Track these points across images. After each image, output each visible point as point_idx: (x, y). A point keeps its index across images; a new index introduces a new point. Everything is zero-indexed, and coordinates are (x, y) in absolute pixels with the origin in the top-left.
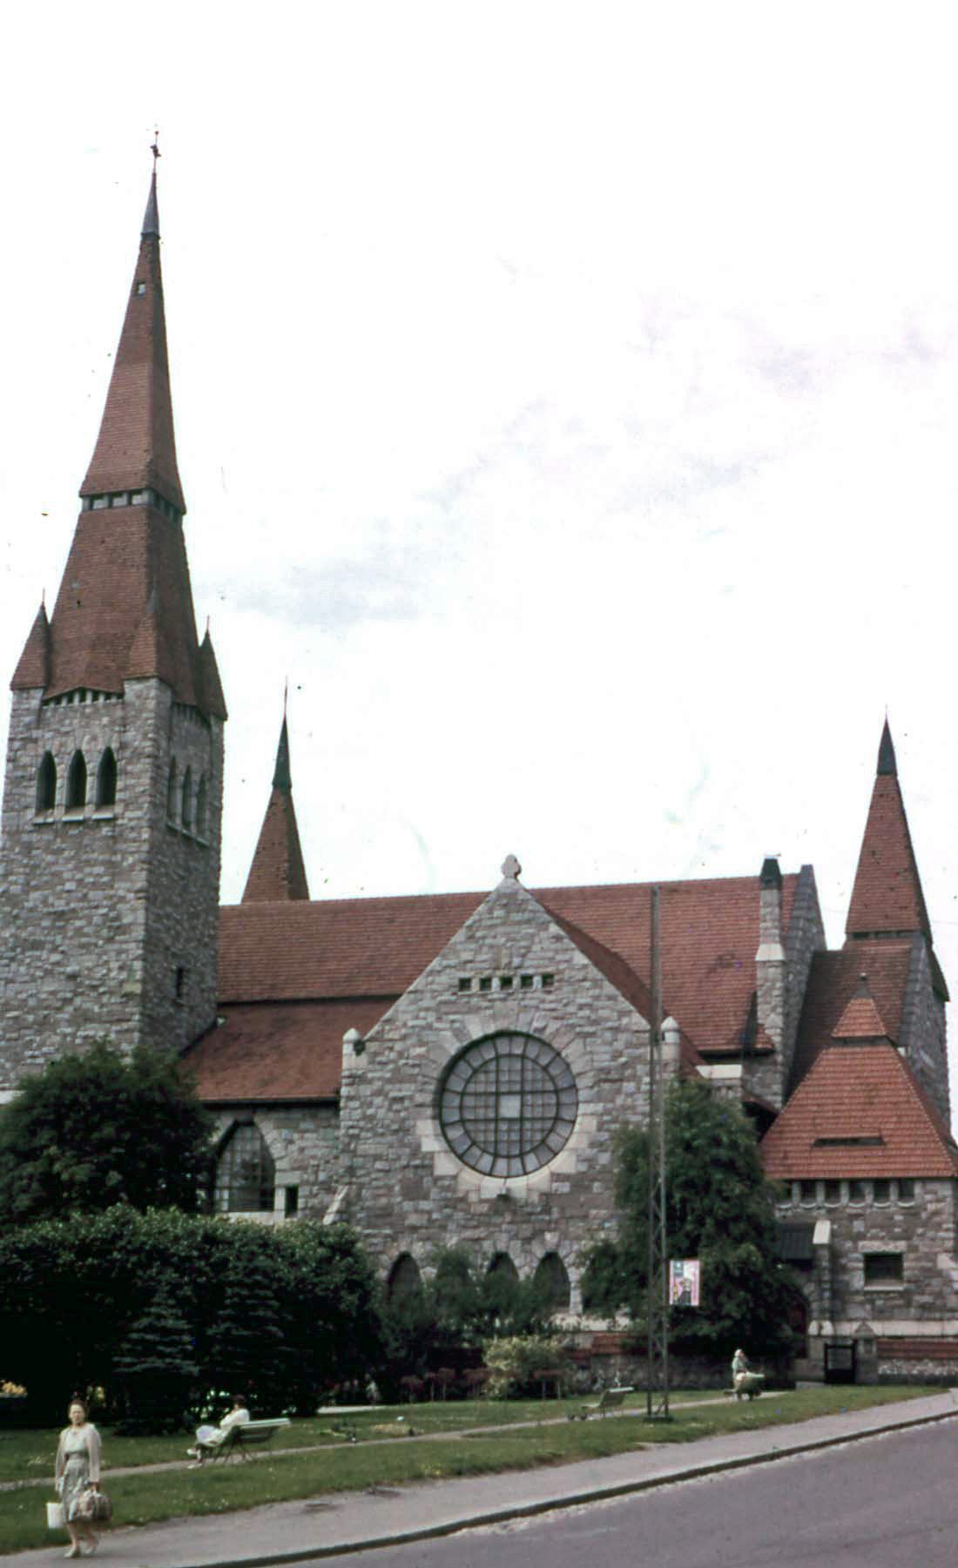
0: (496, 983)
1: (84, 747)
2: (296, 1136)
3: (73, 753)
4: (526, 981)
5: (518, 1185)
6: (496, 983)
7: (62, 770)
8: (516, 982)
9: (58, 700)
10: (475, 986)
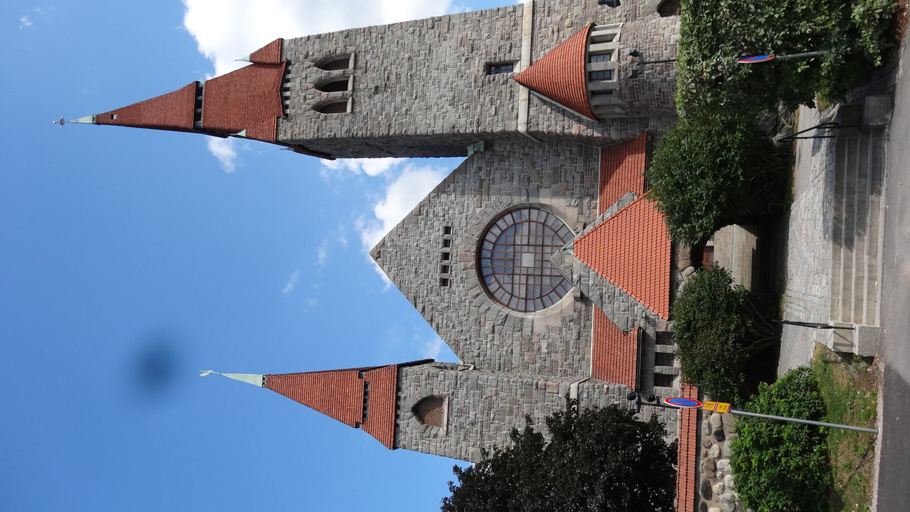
9: (287, 107)
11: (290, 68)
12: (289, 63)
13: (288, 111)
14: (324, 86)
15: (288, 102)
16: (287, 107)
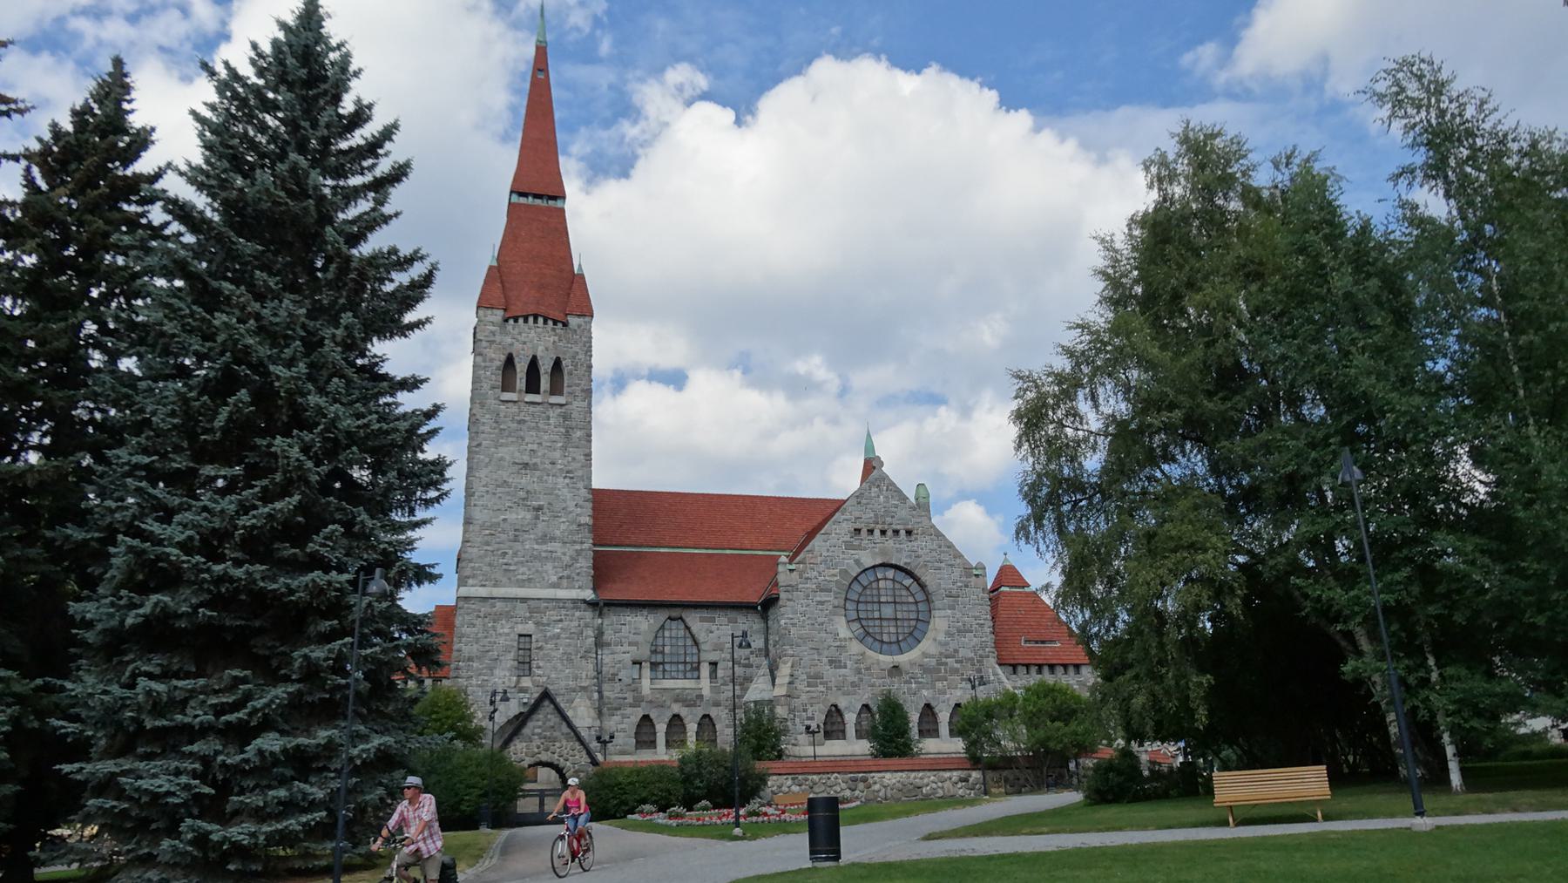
0: (877, 533)
1: (539, 355)
2: (714, 628)
4: (896, 532)
5: (901, 659)
6: (877, 533)
7: (521, 367)
8: (889, 533)
9: (516, 321)
10: (864, 532)
11: (560, 325)
13: (511, 321)
14: (533, 365)
15: (521, 321)
16: (516, 321)
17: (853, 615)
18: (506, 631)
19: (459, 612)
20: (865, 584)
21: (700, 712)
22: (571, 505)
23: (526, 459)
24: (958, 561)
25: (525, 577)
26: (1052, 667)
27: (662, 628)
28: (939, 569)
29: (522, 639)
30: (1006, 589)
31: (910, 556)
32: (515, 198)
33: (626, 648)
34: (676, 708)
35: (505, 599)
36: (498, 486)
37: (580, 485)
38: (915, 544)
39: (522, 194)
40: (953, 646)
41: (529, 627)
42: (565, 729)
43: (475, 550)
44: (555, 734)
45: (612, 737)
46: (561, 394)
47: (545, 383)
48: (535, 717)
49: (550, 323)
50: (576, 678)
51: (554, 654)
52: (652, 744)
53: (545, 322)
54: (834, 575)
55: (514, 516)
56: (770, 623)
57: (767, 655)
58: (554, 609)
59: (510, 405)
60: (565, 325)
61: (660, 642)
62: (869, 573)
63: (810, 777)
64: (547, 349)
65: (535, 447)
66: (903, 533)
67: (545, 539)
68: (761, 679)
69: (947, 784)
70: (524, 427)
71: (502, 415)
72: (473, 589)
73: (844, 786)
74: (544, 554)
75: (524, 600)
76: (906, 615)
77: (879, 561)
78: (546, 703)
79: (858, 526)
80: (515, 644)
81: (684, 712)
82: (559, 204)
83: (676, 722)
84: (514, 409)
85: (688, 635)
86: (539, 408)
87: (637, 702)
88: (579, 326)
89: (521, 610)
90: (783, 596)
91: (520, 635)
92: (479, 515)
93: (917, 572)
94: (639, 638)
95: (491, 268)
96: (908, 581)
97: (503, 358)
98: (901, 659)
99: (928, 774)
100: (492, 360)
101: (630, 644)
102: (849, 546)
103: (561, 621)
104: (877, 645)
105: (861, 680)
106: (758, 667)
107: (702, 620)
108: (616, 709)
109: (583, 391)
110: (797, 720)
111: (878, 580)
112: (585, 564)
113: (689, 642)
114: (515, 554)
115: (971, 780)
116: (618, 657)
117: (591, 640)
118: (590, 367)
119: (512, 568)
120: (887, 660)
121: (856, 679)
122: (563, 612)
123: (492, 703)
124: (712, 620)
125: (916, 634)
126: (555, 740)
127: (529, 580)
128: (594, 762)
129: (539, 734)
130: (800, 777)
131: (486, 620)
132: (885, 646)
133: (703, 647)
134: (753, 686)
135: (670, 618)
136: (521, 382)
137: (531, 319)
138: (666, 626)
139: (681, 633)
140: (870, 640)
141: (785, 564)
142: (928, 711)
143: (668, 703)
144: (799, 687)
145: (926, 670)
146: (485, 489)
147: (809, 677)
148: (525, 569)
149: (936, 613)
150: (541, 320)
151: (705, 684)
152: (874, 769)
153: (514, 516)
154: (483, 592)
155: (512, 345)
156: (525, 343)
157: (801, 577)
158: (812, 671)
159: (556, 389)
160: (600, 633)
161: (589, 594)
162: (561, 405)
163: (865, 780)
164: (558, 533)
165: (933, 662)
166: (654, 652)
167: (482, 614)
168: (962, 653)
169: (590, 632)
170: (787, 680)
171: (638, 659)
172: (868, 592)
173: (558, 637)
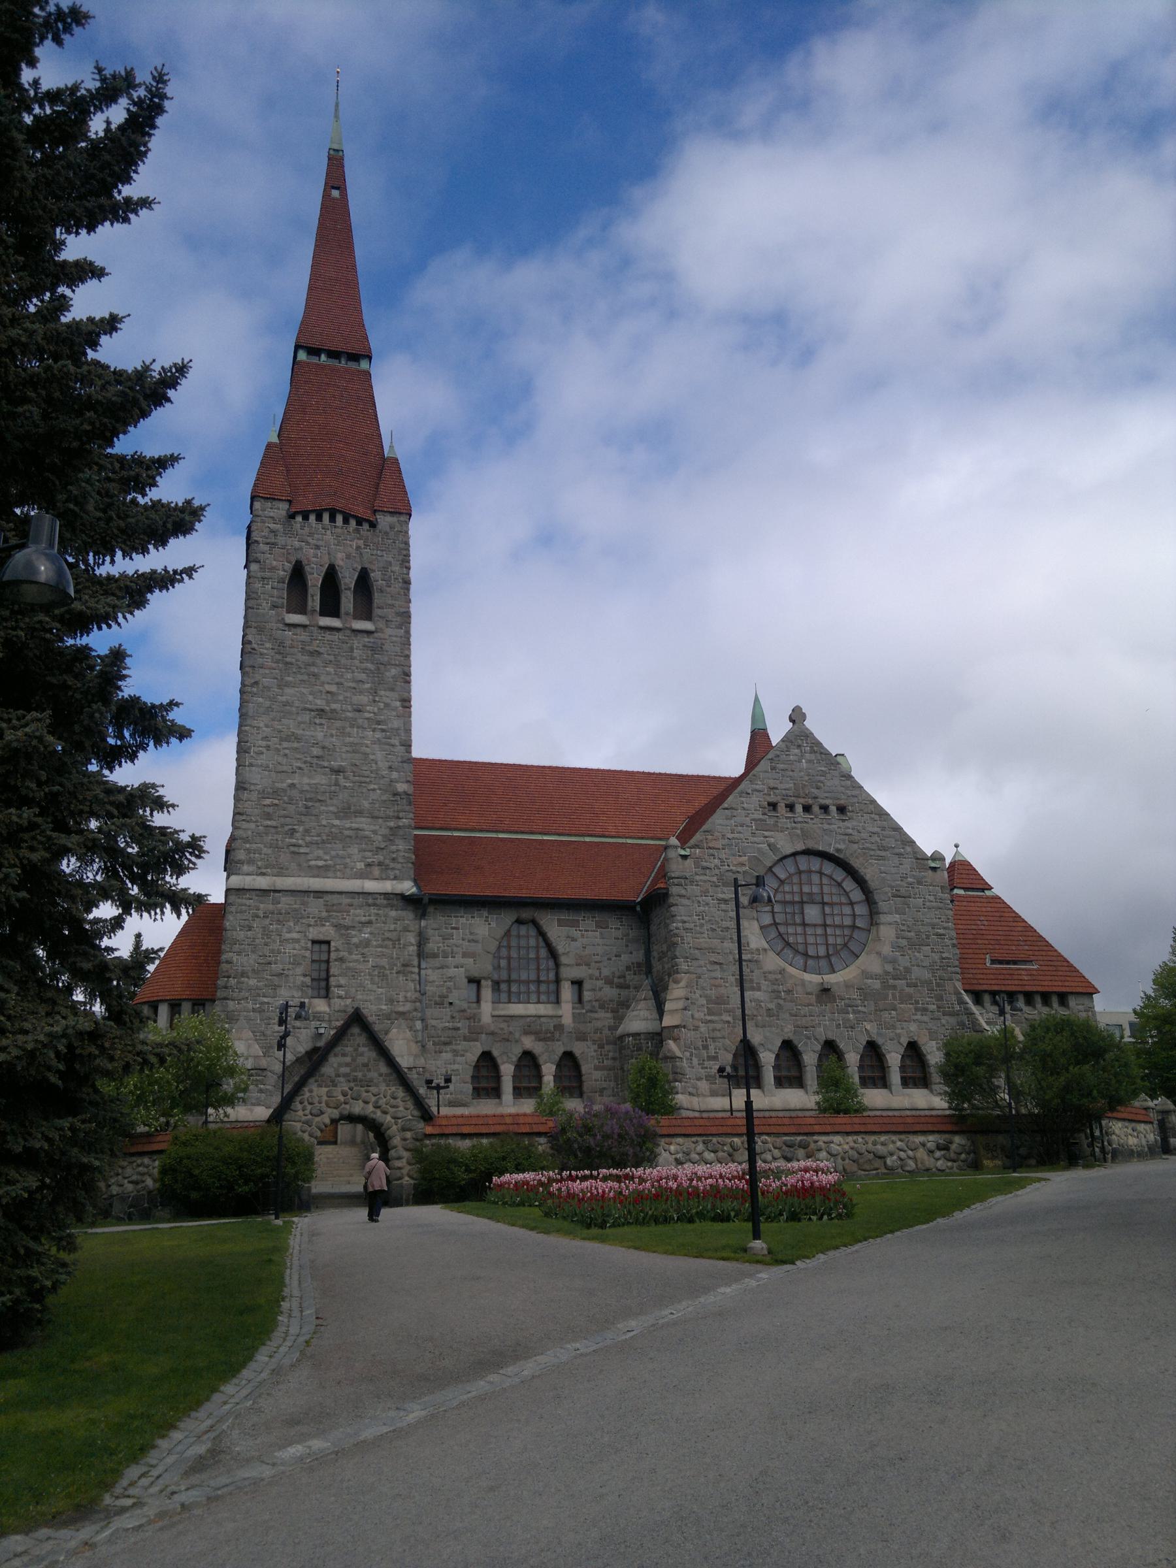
0: (799, 808)
2: (577, 934)
3: (327, 566)
5: (831, 979)
6: (799, 808)
7: (315, 580)
8: (816, 809)
11: (366, 526)
12: (373, 525)
13: (299, 519)
14: (331, 578)
15: (312, 518)
17: (767, 919)
18: (295, 935)
19: (229, 909)
20: (783, 876)
21: (559, 1049)
22: (383, 765)
23: (320, 703)
24: (909, 849)
25: (320, 863)
26: (1029, 997)
27: (508, 934)
28: (883, 858)
29: (316, 947)
30: (961, 892)
31: (844, 841)
32: (302, 356)
33: (459, 959)
34: (528, 1043)
35: (293, 892)
36: (282, 740)
37: (396, 741)
38: (846, 823)
39: (314, 351)
40: (904, 962)
41: (326, 931)
42: (383, 1068)
43: (253, 826)
44: (373, 1075)
45: (448, 1080)
46: (368, 617)
47: (347, 601)
48: (338, 1049)
49: (353, 522)
50: (391, 1001)
51: (361, 967)
52: (496, 1092)
53: (346, 521)
54: (744, 865)
55: (306, 780)
56: (653, 928)
57: (649, 972)
58: (360, 907)
59: (299, 630)
60: (373, 525)
61: (504, 952)
62: (789, 861)
63: (729, 1140)
64: (348, 557)
65: (333, 688)
66: (833, 809)
67: (346, 812)
68: (642, 1005)
69: (921, 1154)
70: (318, 661)
71: (288, 643)
72: (248, 879)
73: (777, 1153)
74: (347, 833)
75: (319, 894)
76: (838, 920)
77: (800, 847)
78: (356, 1030)
79: (772, 799)
80: (308, 954)
81: (537, 1048)
82: (364, 365)
83: (529, 1062)
84: (303, 636)
85: (542, 944)
86: (336, 637)
87: (474, 1034)
88: (392, 527)
89: (315, 907)
90: (674, 890)
91: (314, 942)
92: (256, 777)
93: (856, 863)
94: (478, 948)
95: (269, 446)
96: (839, 874)
97: (289, 567)
98: (831, 979)
99: (894, 1138)
100: (273, 569)
101: (465, 955)
102: (761, 825)
103: (370, 922)
104: (800, 960)
105: (779, 1006)
106: (637, 988)
107: (561, 923)
108: (446, 1044)
109: (398, 614)
110: (695, 1061)
111: (800, 872)
112: (402, 847)
113: (543, 952)
114: (307, 831)
115: (953, 1147)
116: (452, 972)
117: (413, 949)
118: (407, 582)
119: (302, 850)
120: (813, 979)
121: (772, 1006)
122: (373, 910)
123: (282, 1022)
124: (575, 924)
125: (853, 946)
126: (368, 1083)
127: (326, 868)
128: (427, 1116)
129: (345, 1075)
130: (715, 1140)
131: (267, 921)
132: (810, 962)
133: (564, 960)
134: (631, 1014)
135: (519, 922)
136: (315, 600)
137: (326, 516)
138: (514, 933)
139: (532, 942)
140: (789, 953)
141: (676, 847)
142: (873, 1051)
143: (517, 1035)
144: (697, 1015)
145: (865, 993)
146: (264, 743)
147: (709, 1001)
148: (320, 853)
149: (883, 918)
150: (339, 518)
151: (566, 1011)
152: (817, 1128)
153: (306, 780)
154: (262, 882)
155: (301, 549)
156: (318, 547)
157: (697, 865)
158: (713, 993)
159: (365, 608)
160: (422, 940)
161: (408, 887)
162: (369, 633)
163: (804, 1146)
164: (366, 804)
165: (877, 985)
166: (498, 968)
167: (261, 914)
168: (917, 973)
169: (412, 938)
170: (680, 1005)
171: (476, 974)
172: (787, 888)
173: (367, 943)
